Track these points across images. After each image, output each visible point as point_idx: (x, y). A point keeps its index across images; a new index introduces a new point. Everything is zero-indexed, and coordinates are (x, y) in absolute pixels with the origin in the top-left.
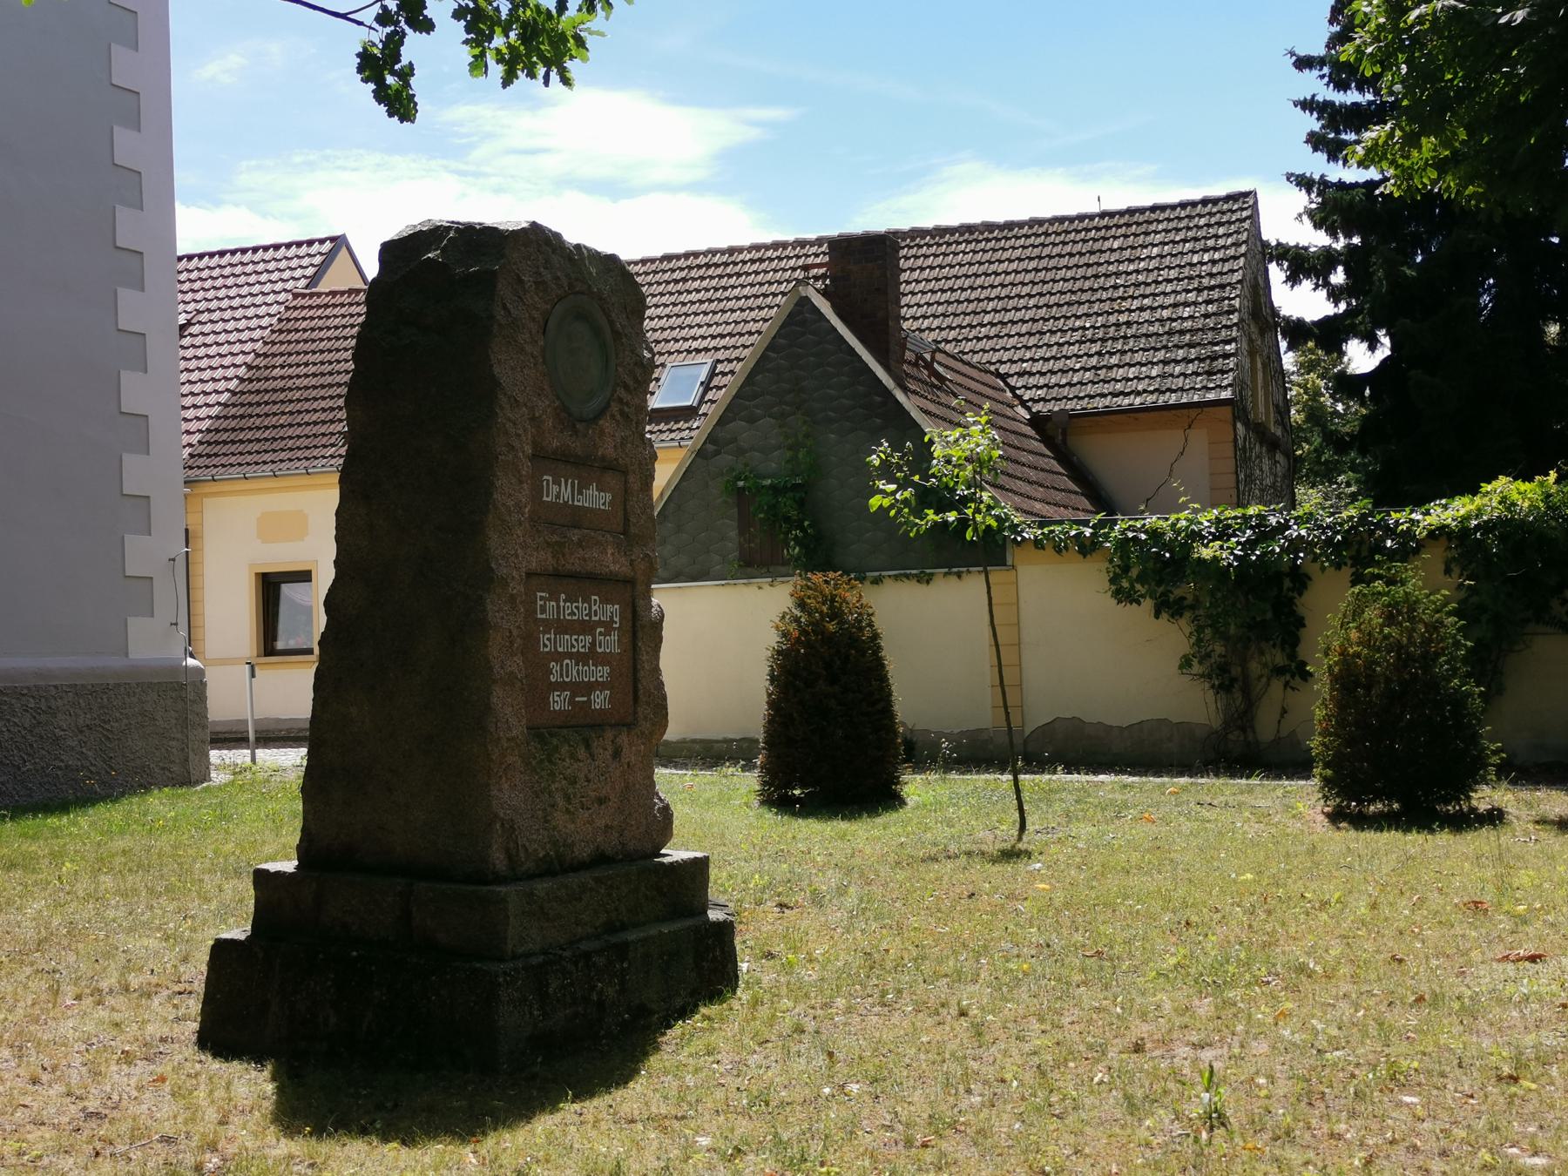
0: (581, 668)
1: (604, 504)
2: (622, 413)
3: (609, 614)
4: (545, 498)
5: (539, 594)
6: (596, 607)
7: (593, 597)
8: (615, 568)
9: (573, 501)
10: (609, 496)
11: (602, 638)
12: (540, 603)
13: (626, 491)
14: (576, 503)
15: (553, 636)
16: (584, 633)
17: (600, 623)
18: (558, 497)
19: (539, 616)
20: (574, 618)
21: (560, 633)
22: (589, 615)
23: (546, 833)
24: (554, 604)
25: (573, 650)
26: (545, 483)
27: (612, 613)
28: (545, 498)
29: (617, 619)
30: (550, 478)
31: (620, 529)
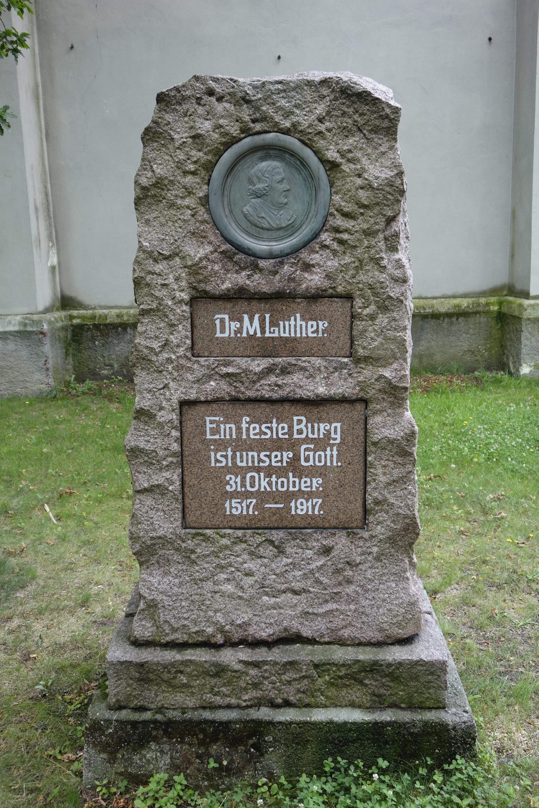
0: (274, 479)
1: (317, 331)
2: (341, 242)
3: (322, 430)
4: (218, 335)
5: (208, 419)
6: (302, 426)
7: (295, 418)
8: (322, 390)
9: (263, 331)
10: (323, 325)
11: (311, 454)
12: (209, 426)
13: (352, 317)
14: (267, 335)
15: (230, 453)
16: (280, 449)
17: (307, 440)
18: (239, 331)
19: (209, 437)
20: (263, 437)
21: (241, 451)
22: (290, 432)
23: (202, 614)
24: (233, 426)
25: (261, 464)
26: (218, 322)
27: (329, 431)
28: (218, 335)
29: (338, 436)
30: (226, 317)
31: (346, 350)
